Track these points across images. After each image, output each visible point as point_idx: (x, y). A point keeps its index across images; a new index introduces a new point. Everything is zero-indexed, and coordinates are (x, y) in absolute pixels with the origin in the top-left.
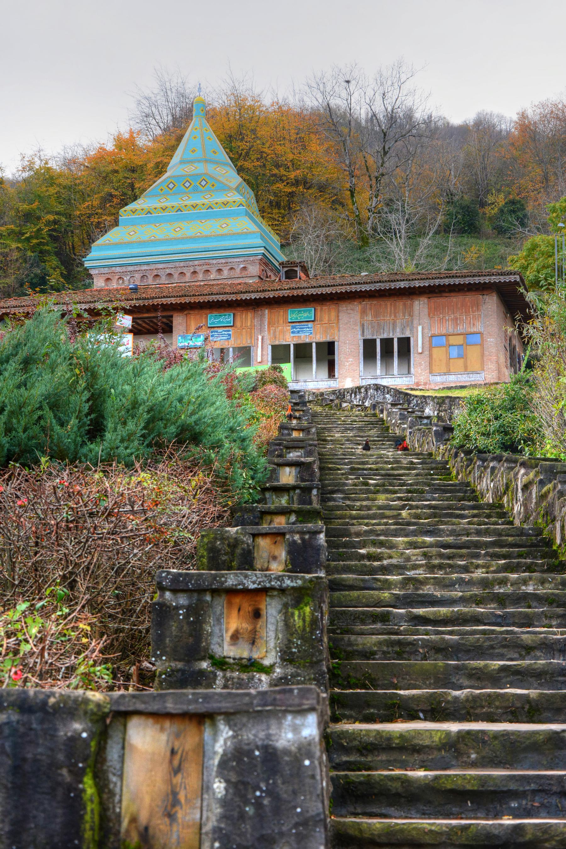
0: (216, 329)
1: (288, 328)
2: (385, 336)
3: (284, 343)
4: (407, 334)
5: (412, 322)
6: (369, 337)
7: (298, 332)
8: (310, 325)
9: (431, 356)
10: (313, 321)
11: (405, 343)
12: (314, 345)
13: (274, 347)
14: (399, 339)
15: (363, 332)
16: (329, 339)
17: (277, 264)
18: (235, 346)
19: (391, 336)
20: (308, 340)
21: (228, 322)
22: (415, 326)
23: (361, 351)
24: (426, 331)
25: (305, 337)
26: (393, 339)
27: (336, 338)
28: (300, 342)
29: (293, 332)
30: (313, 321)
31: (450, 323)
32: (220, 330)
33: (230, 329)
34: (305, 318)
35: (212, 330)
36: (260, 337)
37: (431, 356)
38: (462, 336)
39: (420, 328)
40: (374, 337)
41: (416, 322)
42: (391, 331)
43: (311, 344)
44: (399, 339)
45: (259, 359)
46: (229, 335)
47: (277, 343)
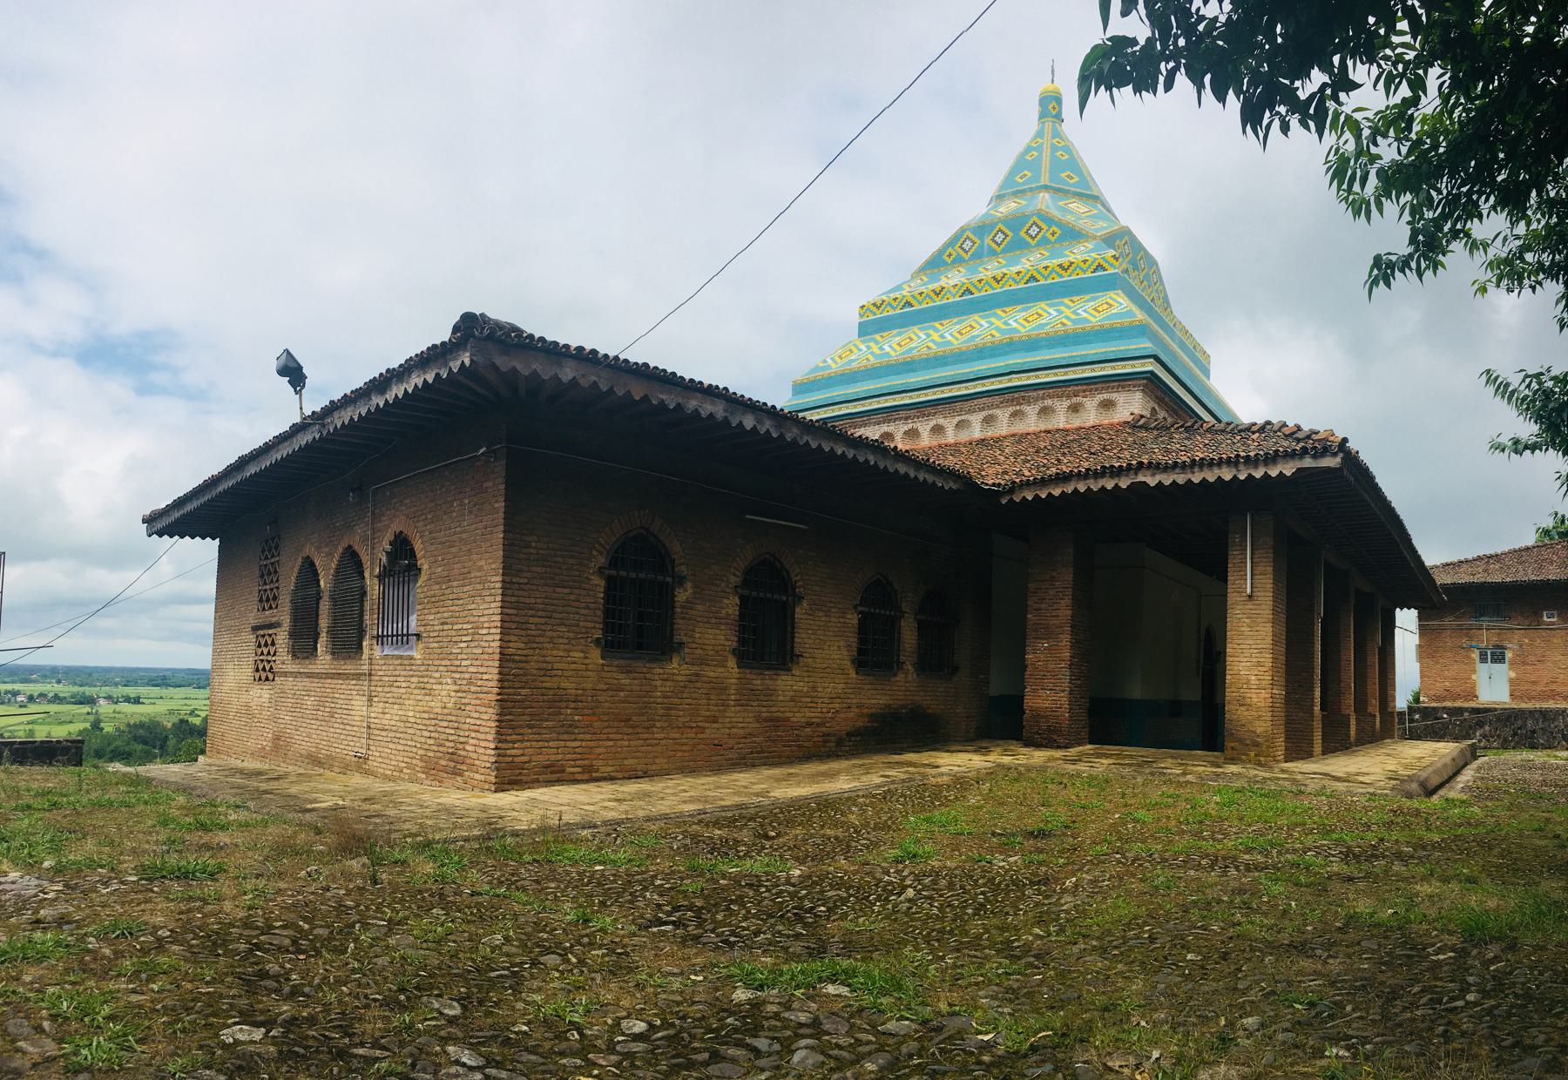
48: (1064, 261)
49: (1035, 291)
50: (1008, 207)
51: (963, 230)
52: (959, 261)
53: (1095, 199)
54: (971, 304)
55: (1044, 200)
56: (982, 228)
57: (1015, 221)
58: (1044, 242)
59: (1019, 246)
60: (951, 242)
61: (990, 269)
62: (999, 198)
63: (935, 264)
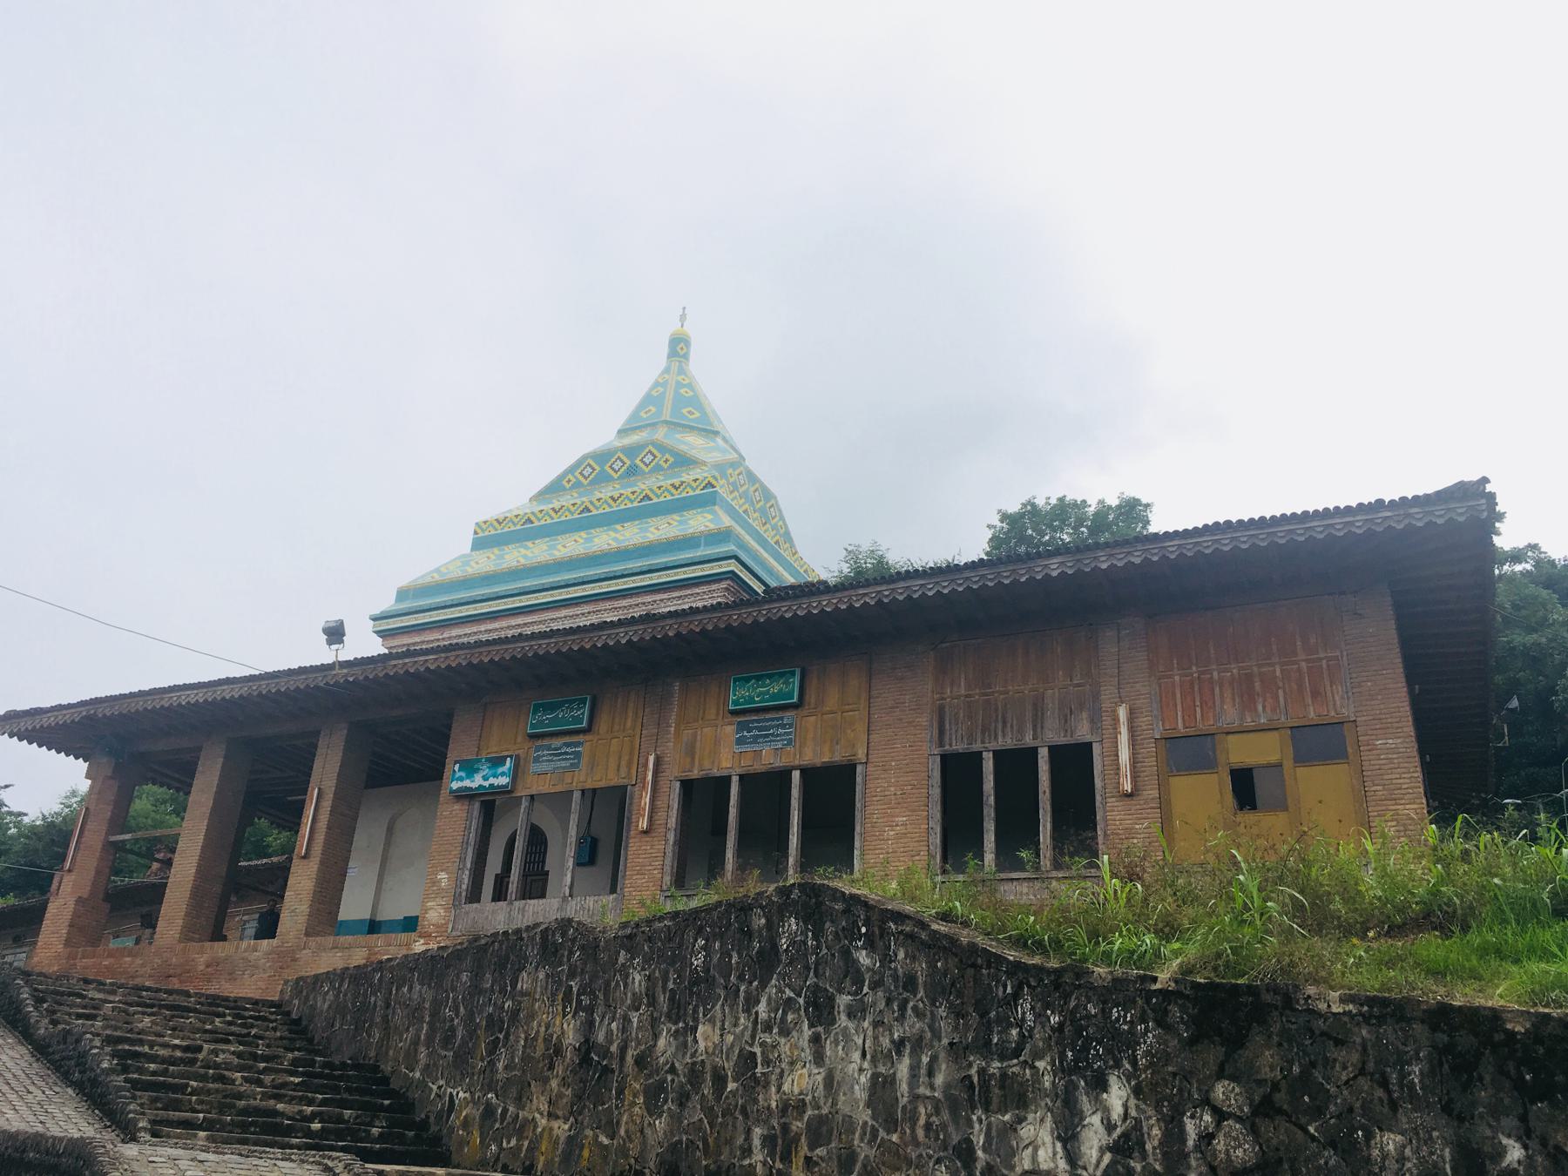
0: (546, 742)
1: (730, 729)
2: (1007, 742)
3: (716, 772)
4: (1083, 733)
5: (1096, 696)
6: (959, 746)
7: (755, 739)
8: (788, 716)
9: (1164, 806)
10: (795, 706)
11: (1075, 763)
12: (796, 775)
13: (687, 786)
14: (1053, 750)
15: (941, 732)
16: (838, 756)
17: (759, 588)
18: (589, 785)
19: (1028, 740)
20: (780, 763)
21: (578, 720)
22: (1106, 705)
23: (936, 792)
24: (1143, 721)
25: (768, 757)
26: (1033, 752)
27: (861, 754)
28: (758, 767)
29: (740, 741)
30: (795, 706)
31: (1228, 694)
32: (557, 742)
33: (580, 738)
34: (774, 697)
35: (539, 743)
36: (652, 759)
37: (1164, 806)
38: (1276, 733)
39: (1122, 713)
40: (977, 747)
41: (1108, 693)
42: (1029, 726)
43: (785, 774)
44: (1053, 750)
45: (643, 824)
46: (578, 755)
47: (695, 774)
48: (677, 482)
49: (647, 510)
50: (628, 441)
51: (585, 457)
52: (578, 485)
53: (710, 433)
54: (587, 521)
55: (660, 434)
56: (602, 457)
57: (631, 451)
58: (658, 469)
59: (633, 471)
60: (571, 470)
61: (606, 492)
62: (622, 432)
63: (554, 488)
